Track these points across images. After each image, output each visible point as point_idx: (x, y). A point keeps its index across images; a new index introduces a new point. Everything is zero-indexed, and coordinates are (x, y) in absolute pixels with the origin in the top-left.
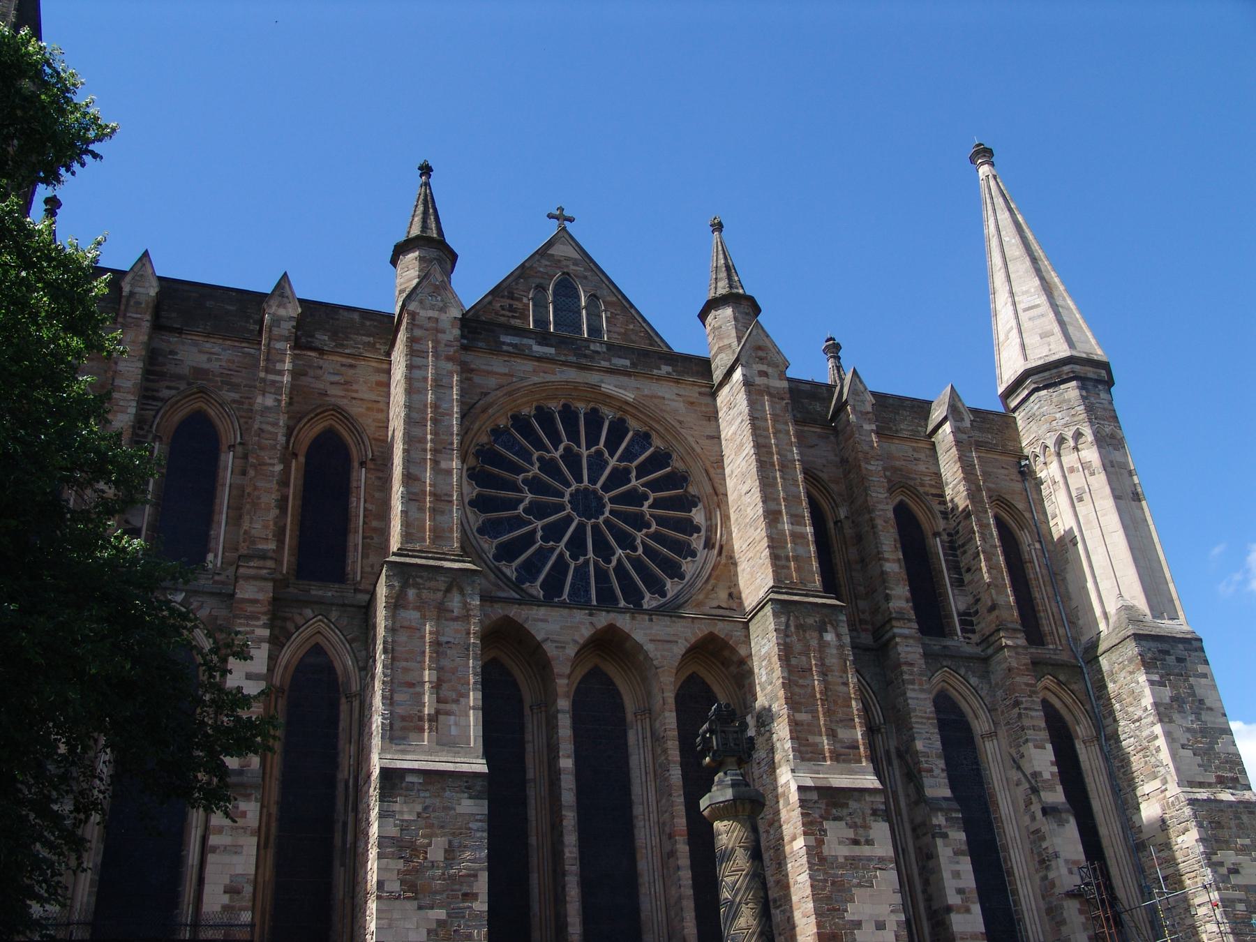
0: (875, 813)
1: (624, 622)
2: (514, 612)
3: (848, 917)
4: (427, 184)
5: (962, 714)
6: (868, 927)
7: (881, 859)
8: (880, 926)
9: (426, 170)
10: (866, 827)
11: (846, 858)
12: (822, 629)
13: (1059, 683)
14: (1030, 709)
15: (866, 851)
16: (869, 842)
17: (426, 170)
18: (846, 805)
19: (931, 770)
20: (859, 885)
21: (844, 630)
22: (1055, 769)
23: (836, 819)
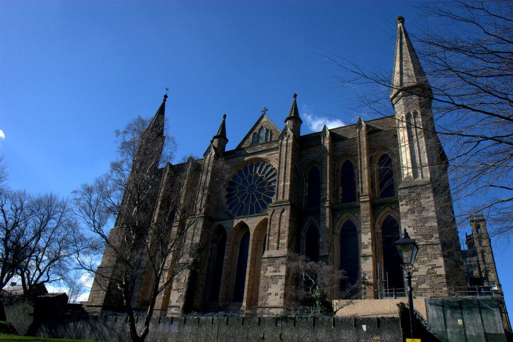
0: (282, 263)
1: (245, 220)
2: (221, 223)
3: (268, 292)
4: (224, 121)
5: (354, 226)
6: (273, 294)
7: (281, 276)
8: (276, 294)
9: (225, 116)
10: (279, 267)
11: (271, 276)
12: (283, 211)
13: (392, 209)
14: (365, 222)
15: (277, 274)
16: (279, 271)
17: (225, 116)
18: (275, 262)
19: (324, 247)
20: (274, 283)
21: (289, 211)
22: (370, 241)
23: (270, 265)
